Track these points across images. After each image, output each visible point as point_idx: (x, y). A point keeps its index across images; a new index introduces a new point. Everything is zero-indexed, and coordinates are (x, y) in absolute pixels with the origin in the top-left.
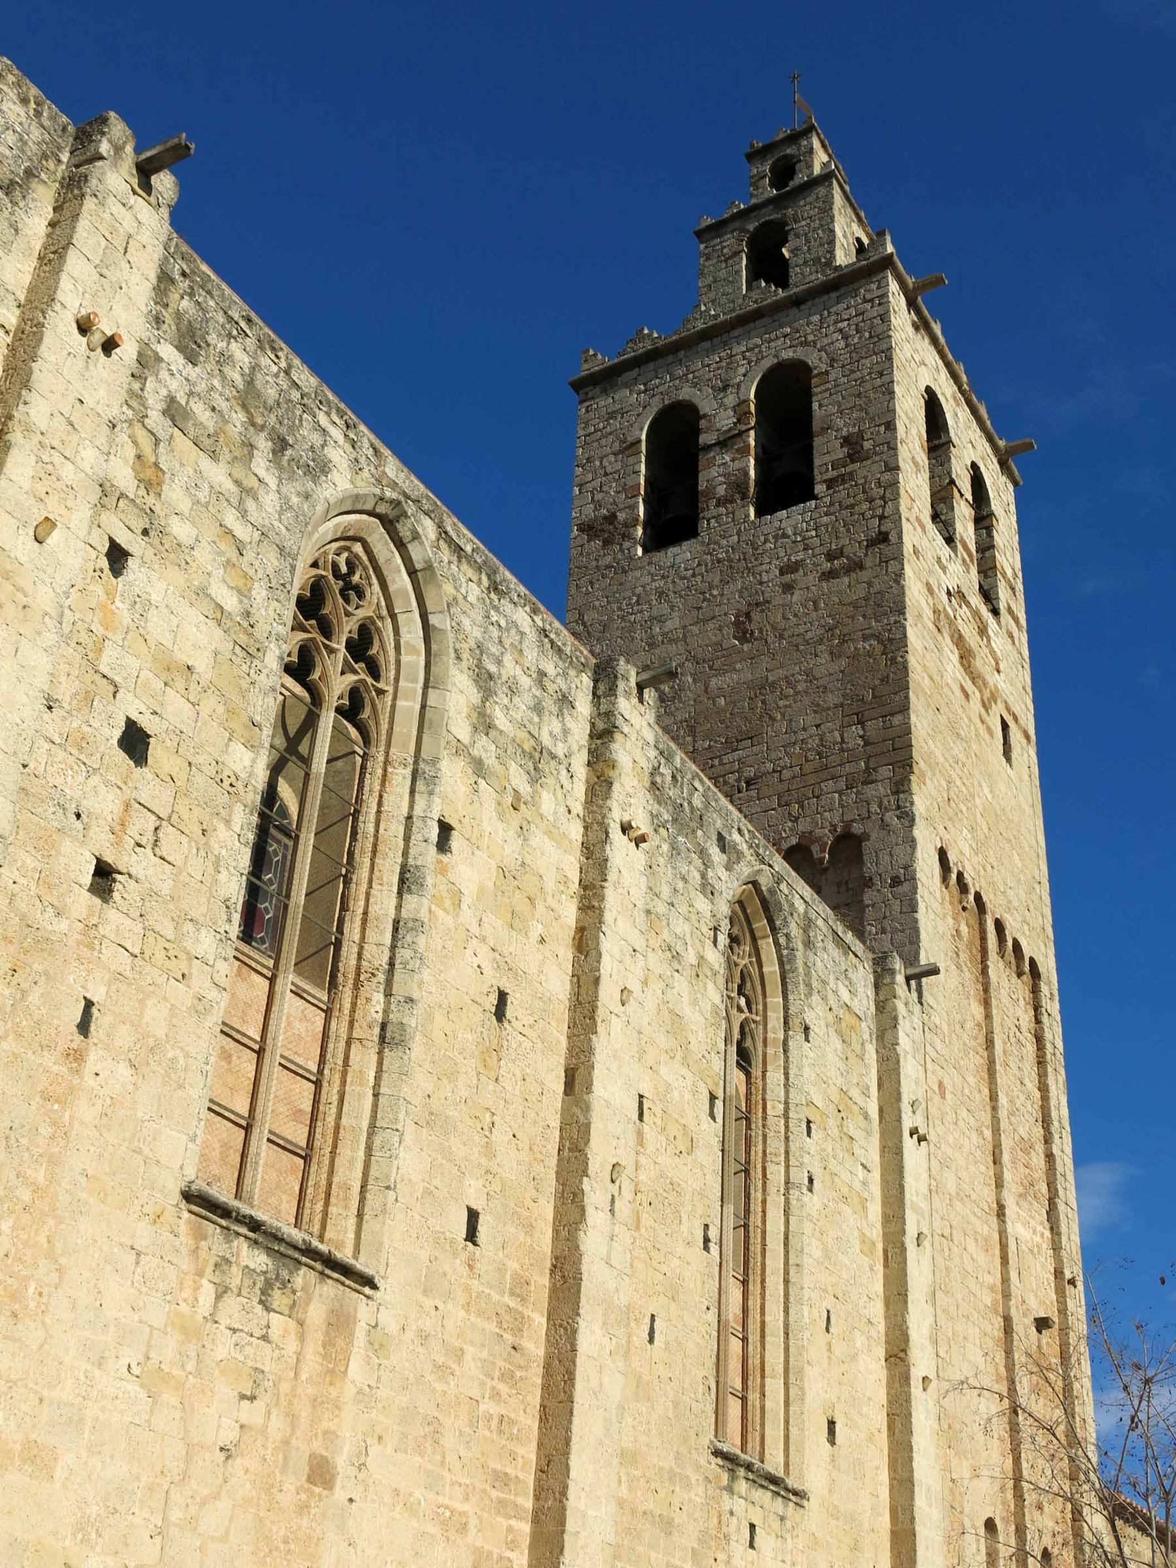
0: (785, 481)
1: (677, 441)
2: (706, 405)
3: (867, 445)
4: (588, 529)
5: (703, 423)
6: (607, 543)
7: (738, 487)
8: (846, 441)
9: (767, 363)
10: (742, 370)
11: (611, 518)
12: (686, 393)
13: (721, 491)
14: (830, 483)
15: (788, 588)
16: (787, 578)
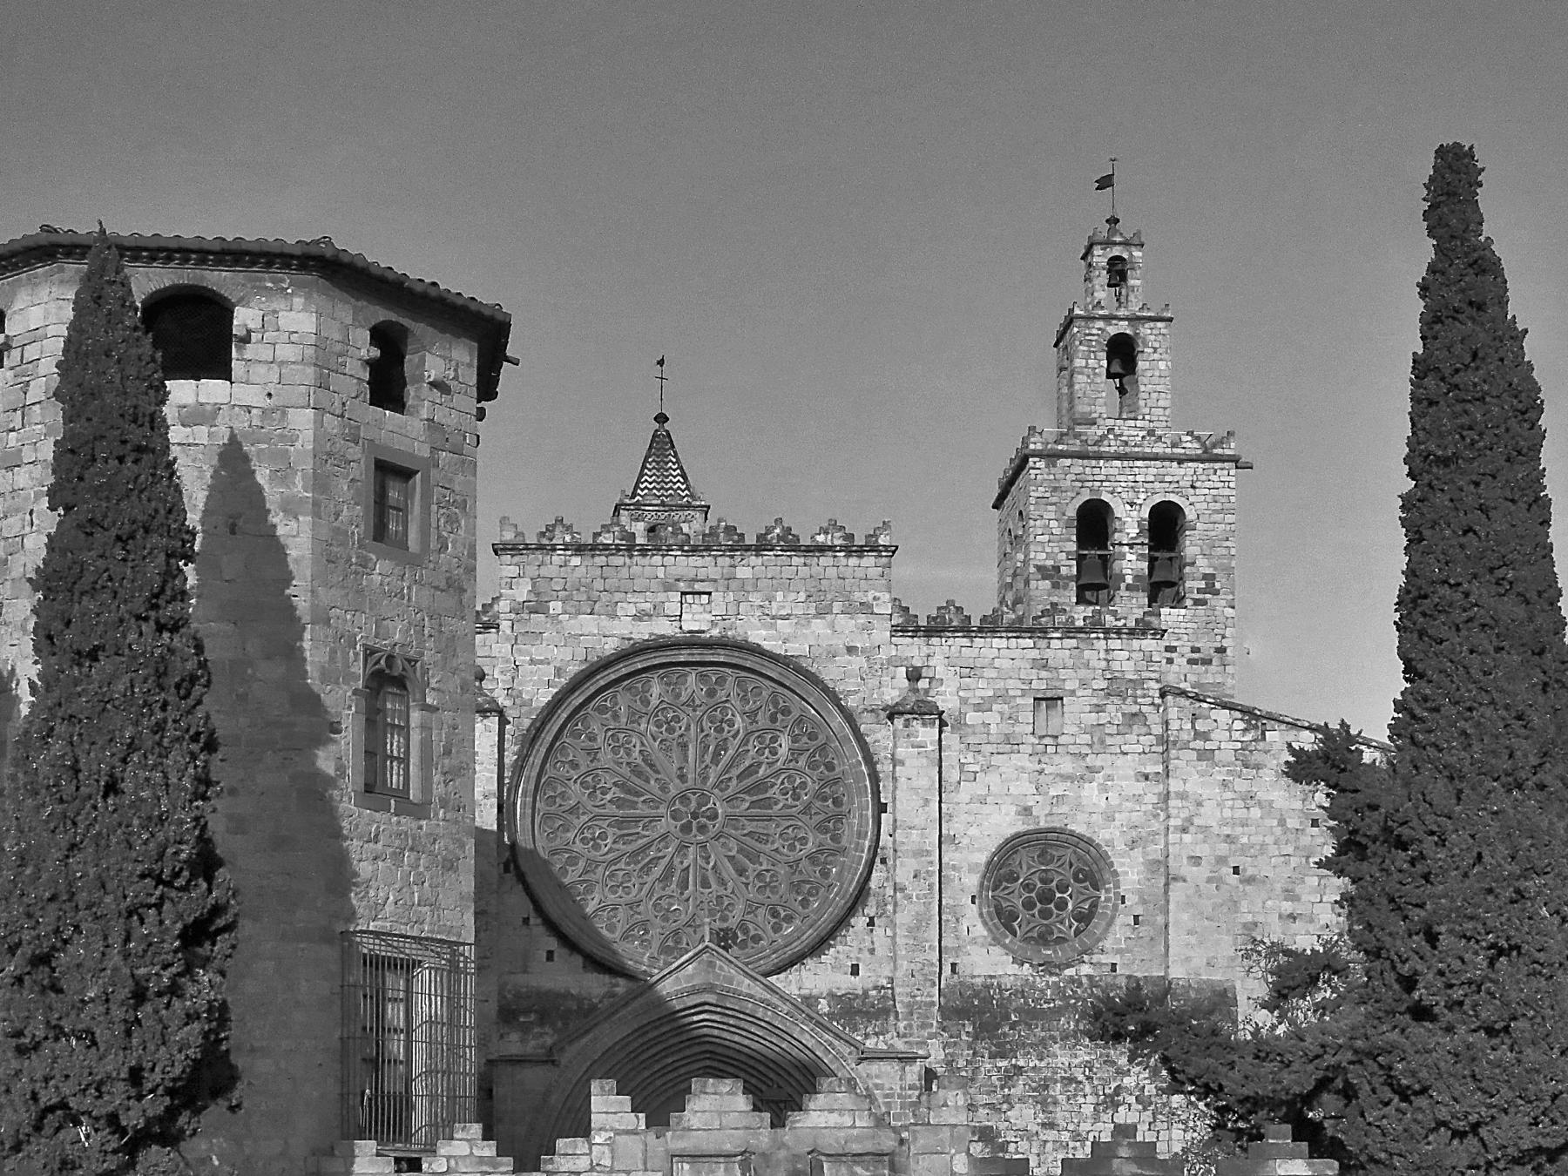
0: (1163, 586)
1: (1094, 523)
2: (1119, 509)
3: (1218, 586)
4: (1039, 568)
5: (1117, 524)
6: (1055, 586)
7: (1136, 578)
8: (1205, 577)
9: (1158, 499)
10: (1142, 496)
11: (1057, 569)
12: (1105, 497)
13: (1129, 579)
14: (1197, 602)
15: (1170, 661)
16: (1168, 655)
